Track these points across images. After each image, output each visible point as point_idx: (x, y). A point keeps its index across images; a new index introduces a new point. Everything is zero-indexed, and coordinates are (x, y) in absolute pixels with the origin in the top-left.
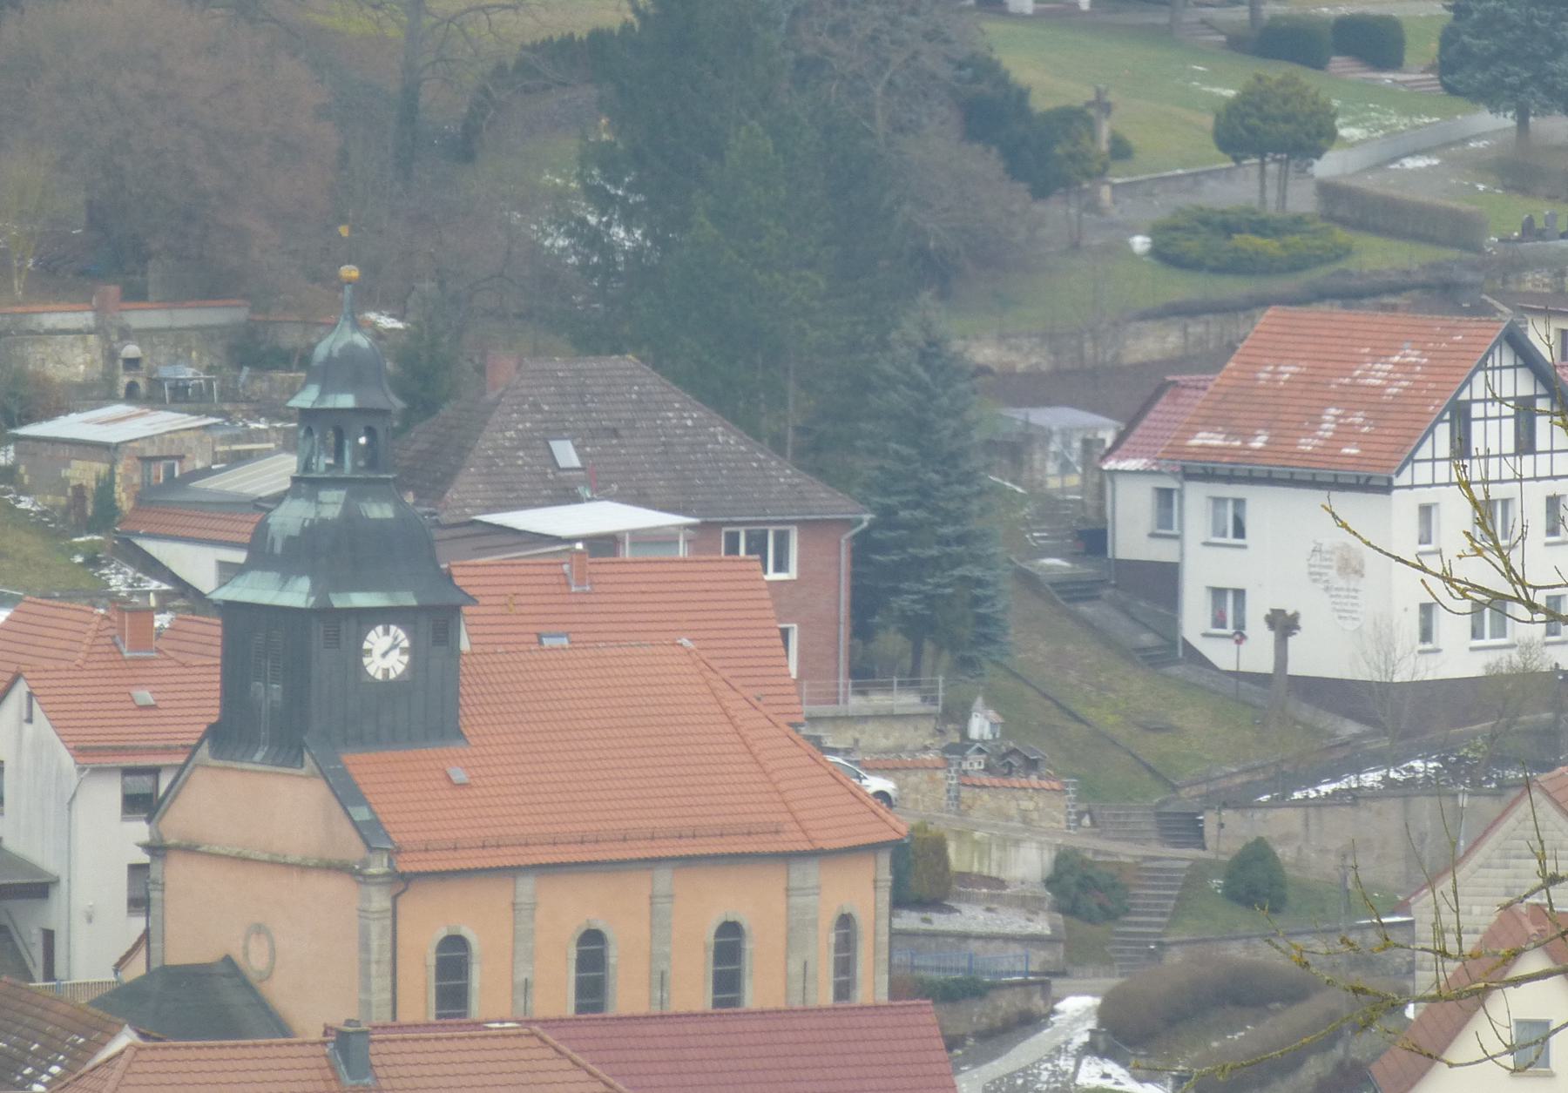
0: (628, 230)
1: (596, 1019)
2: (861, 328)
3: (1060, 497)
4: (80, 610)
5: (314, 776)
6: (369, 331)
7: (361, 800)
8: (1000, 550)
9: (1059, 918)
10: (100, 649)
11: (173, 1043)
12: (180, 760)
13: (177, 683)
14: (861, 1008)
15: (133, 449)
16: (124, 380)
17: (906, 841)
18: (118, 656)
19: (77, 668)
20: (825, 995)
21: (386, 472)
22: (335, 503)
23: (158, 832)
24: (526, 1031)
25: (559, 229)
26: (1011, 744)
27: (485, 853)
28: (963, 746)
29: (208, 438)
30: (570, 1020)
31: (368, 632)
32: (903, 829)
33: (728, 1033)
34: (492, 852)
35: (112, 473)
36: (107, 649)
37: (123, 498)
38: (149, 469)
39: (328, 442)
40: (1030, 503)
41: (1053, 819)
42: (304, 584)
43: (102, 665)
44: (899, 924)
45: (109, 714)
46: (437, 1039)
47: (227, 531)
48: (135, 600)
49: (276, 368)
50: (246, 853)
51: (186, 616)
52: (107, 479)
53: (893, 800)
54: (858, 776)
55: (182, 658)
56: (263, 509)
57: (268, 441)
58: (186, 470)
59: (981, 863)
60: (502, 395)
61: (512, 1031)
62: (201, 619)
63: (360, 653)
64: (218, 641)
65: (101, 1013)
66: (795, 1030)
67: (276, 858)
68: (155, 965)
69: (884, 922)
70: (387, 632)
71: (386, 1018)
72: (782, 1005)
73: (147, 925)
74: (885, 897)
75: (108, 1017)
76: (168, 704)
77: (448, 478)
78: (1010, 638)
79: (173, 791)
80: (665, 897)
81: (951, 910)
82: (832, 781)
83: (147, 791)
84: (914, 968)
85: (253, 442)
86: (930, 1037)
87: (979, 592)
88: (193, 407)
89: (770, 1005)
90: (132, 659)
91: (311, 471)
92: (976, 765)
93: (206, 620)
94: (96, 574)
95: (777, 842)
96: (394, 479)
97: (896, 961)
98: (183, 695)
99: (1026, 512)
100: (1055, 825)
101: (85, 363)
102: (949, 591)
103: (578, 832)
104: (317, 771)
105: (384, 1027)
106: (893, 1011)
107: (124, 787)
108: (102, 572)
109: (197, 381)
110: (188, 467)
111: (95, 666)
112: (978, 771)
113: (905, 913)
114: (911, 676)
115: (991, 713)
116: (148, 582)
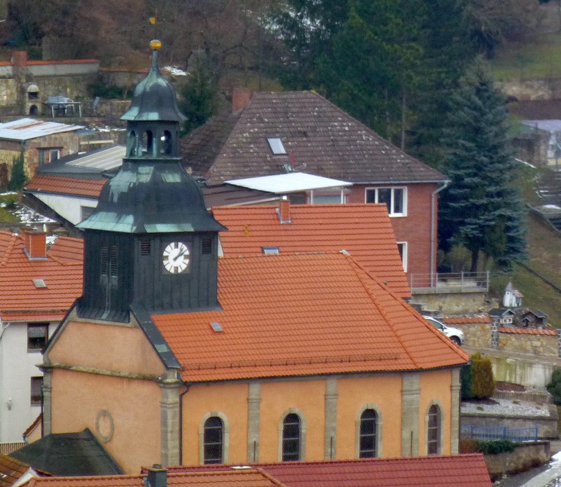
0: (312, 20)
1: (294, 464)
2: (443, 75)
3: (555, 170)
4: (4, 234)
5: (135, 327)
6: (167, 77)
7: (162, 341)
8: (521, 200)
9: (555, 407)
10: (15, 256)
11: (56, 478)
12: (61, 318)
13: (59, 275)
14: (443, 458)
15: (34, 143)
16: (29, 104)
17: (469, 364)
18: (26, 260)
19: (2, 267)
20: (424, 451)
21: (176, 156)
22: (147, 174)
23: (48, 359)
24: (255, 471)
25: (273, 19)
26: (528, 310)
27: (231, 370)
28: (500, 311)
29: (76, 137)
30: (279, 465)
31: (167, 246)
32: (467, 357)
33: (368, 472)
34: (236, 370)
35: (22, 157)
36: (19, 256)
37: (28, 171)
38: (43, 155)
39: (143, 139)
40: (538, 174)
41: (551, 352)
42: (130, 219)
43: (17, 265)
44: (465, 410)
45: (21, 292)
46: (205, 475)
47: (87, 189)
48: (35, 228)
49: (114, 98)
50: (97, 370)
51: (64, 238)
52: (19, 160)
53: (461, 341)
54: (442, 328)
55: (62, 261)
56: (107, 177)
57: (110, 139)
58: (64, 155)
59: (510, 376)
60: (241, 113)
61: (247, 471)
62: (73, 239)
63: (162, 258)
64: (82, 251)
65: (16, 460)
66: (406, 470)
67: (114, 373)
68: (46, 434)
69: (456, 410)
70: (176, 246)
71: (176, 464)
72: (399, 456)
73: (42, 411)
74: (457, 395)
75: (20, 463)
76: (53, 287)
77: (211, 160)
78: (527, 250)
79: (57, 336)
80: (334, 395)
81: (494, 403)
82: (427, 330)
83: (42, 336)
84: (473, 435)
85: (102, 139)
86: (482, 474)
87: (509, 224)
88: (68, 119)
89: (392, 456)
90: (34, 262)
91: (134, 156)
92: (508, 322)
93: (75, 239)
94: (13, 214)
95: (396, 364)
96: (181, 160)
97: (463, 431)
98: (62, 282)
99: (536, 178)
100: (552, 355)
101: (7, 95)
102: (493, 223)
103: (284, 359)
104: (138, 325)
105: (175, 469)
106: (462, 460)
107: (29, 333)
108: (16, 212)
109: (70, 105)
110: (65, 153)
111: (13, 265)
112: (509, 324)
113: (468, 404)
114: (471, 271)
115: (516, 292)
116: (42, 218)
